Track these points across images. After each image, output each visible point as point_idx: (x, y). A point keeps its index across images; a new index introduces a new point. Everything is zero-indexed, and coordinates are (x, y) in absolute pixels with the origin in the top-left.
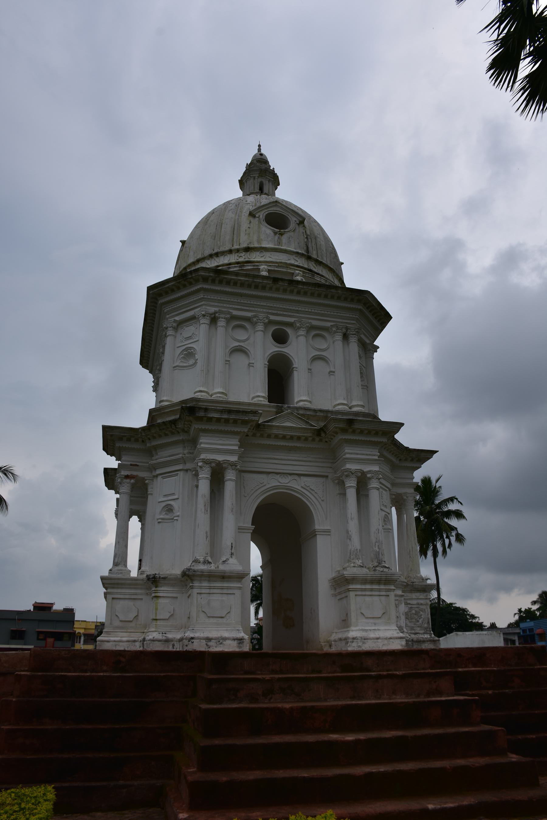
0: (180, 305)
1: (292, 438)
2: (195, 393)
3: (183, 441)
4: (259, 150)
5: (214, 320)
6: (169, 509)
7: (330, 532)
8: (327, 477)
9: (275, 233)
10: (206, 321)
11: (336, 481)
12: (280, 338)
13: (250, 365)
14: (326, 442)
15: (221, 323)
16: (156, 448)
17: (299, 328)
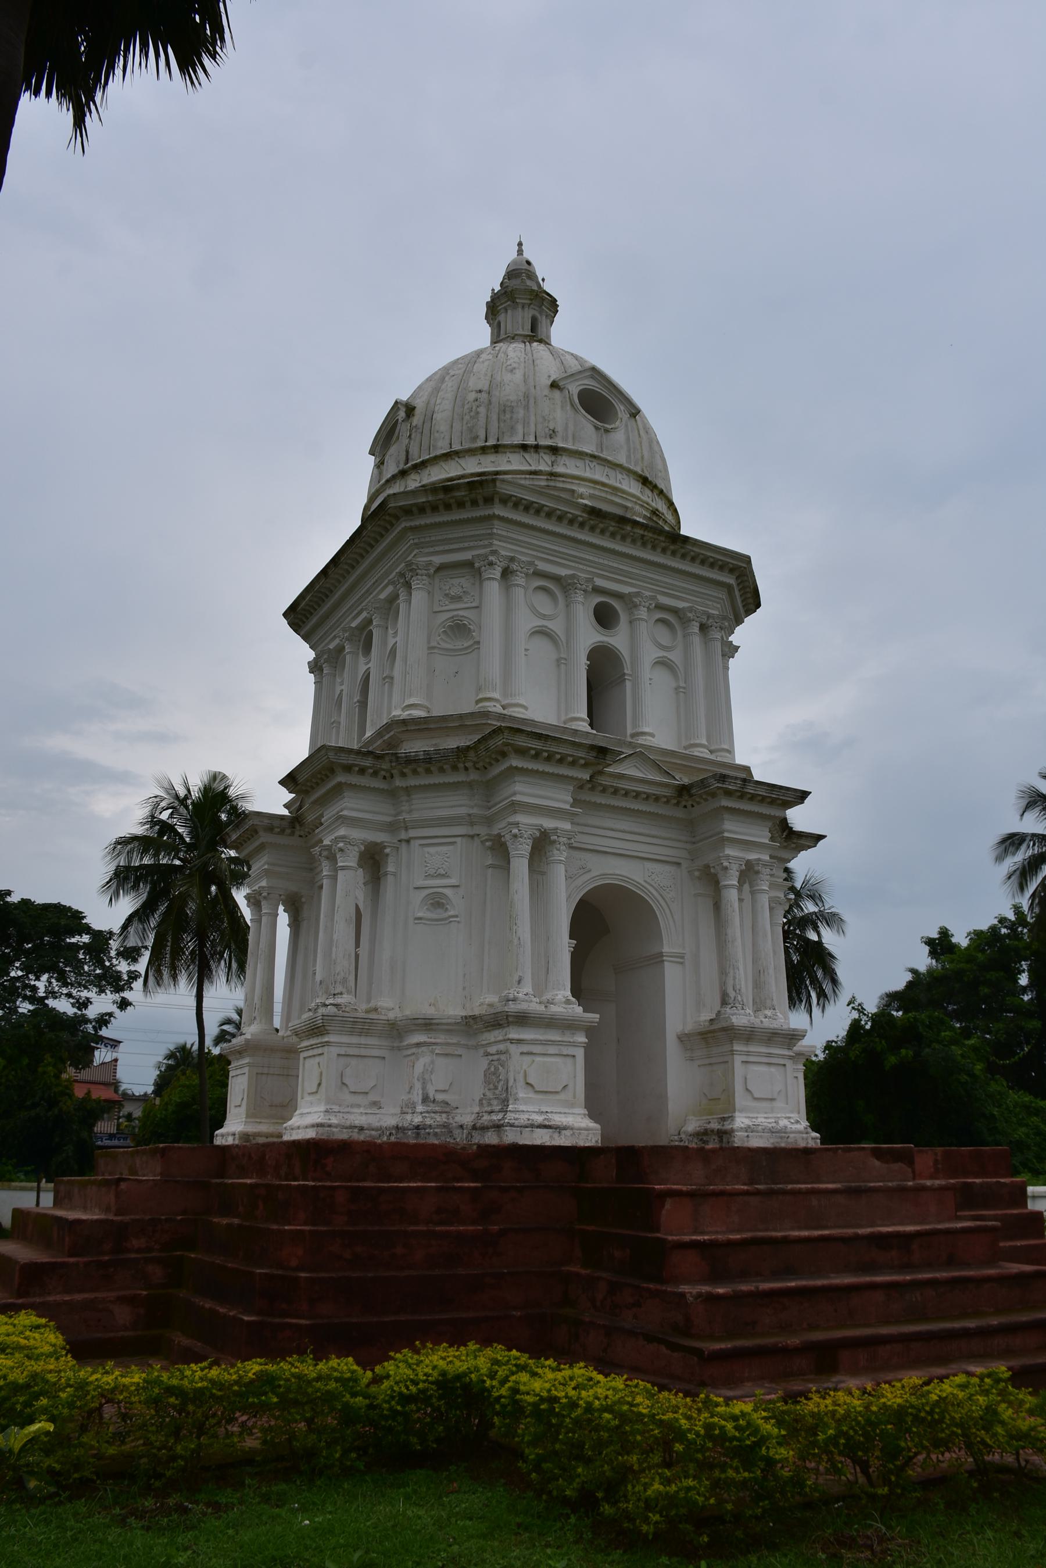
0: (450, 536)
1: (637, 795)
2: (478, 702)
3: (470, 785)
4: (520, 252)
5: (506, 573)
6: (437, 902)
7: (682, 958)
8: (679, 864)
9: (597, 428)
10: (497, 573)
11: (697, 874)
12: (604, 617)
13: (558, 661)
14: (685, 807)
15: (520, 580)
16: (408, 790)
17: (636, 606)
